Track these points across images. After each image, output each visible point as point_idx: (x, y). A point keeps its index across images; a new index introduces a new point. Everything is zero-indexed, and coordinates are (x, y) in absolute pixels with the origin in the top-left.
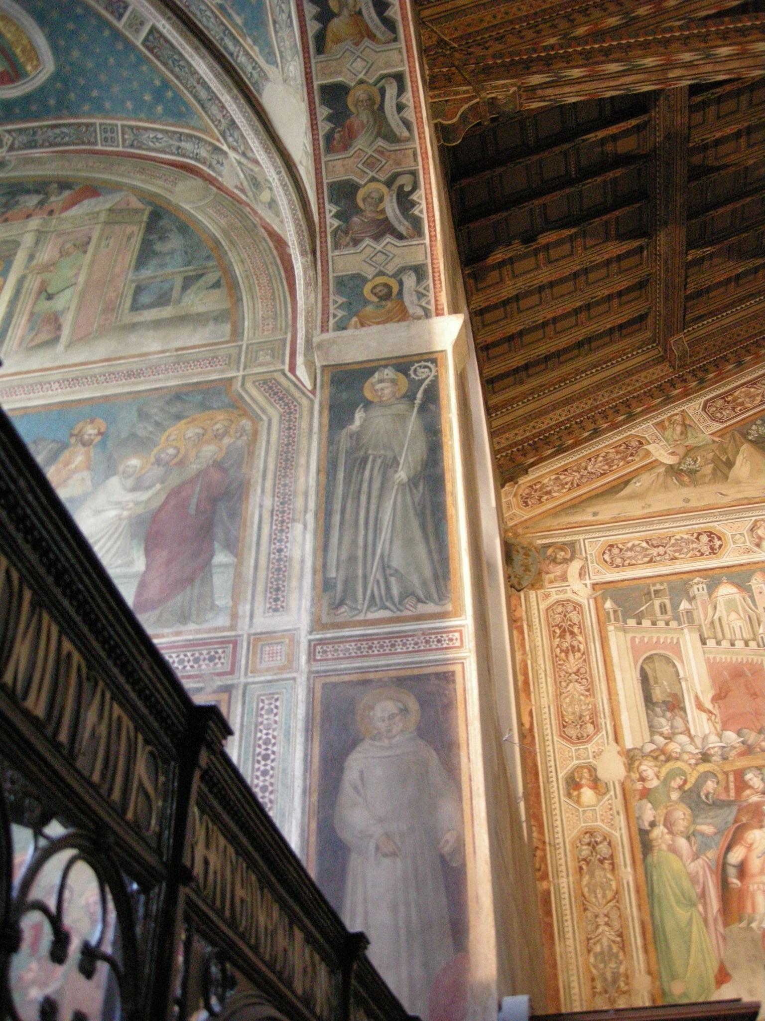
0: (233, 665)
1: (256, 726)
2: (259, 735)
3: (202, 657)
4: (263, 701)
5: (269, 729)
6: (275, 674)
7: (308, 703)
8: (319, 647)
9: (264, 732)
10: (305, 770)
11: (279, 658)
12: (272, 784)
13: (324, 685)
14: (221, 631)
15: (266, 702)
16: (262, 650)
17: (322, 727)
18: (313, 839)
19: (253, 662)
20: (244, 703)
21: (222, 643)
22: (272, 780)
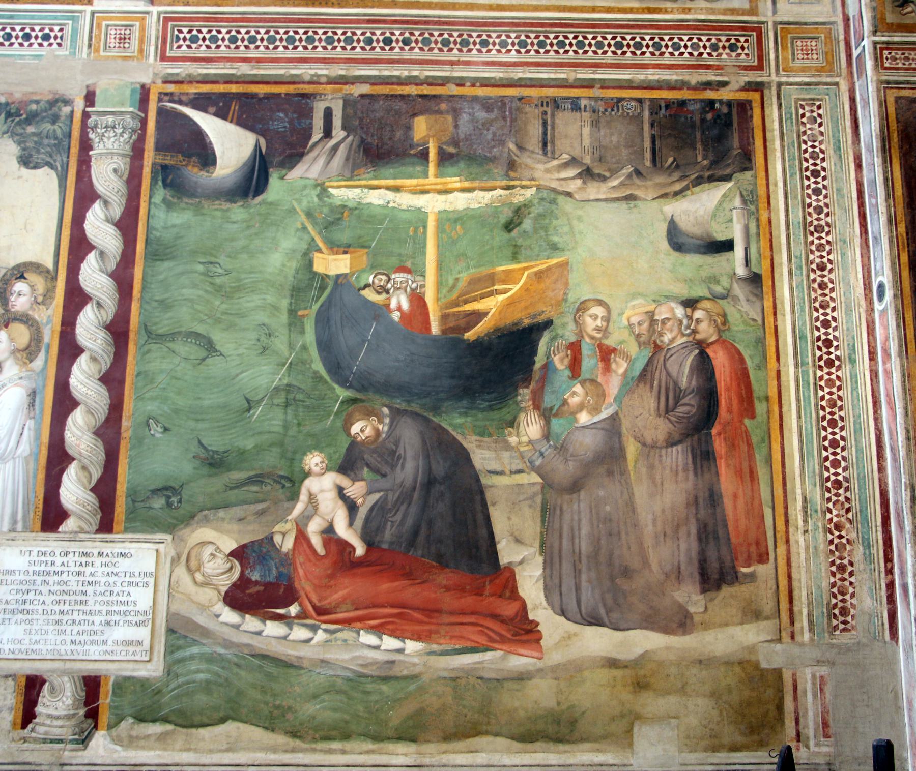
0: (760, 58)
1: (799, 137)
2: (804, 147)
3: (721, 44)
4: (802, 107)
5: (815, 141)
6: (813, 76)
7: (881, 119)
8: (886, 52)
9: (810, 144)
10: (888, 196)
11: (815, 57)
12: (827, 205)
13: (897, 99)
14: (738, 15)
15: (807, 108)
16: (792, 44)
17: (901, 148)
18: (906, 273)
19: (785, 59)
20: (780, 106)
21: (743, 29)
22: (827, 201)
